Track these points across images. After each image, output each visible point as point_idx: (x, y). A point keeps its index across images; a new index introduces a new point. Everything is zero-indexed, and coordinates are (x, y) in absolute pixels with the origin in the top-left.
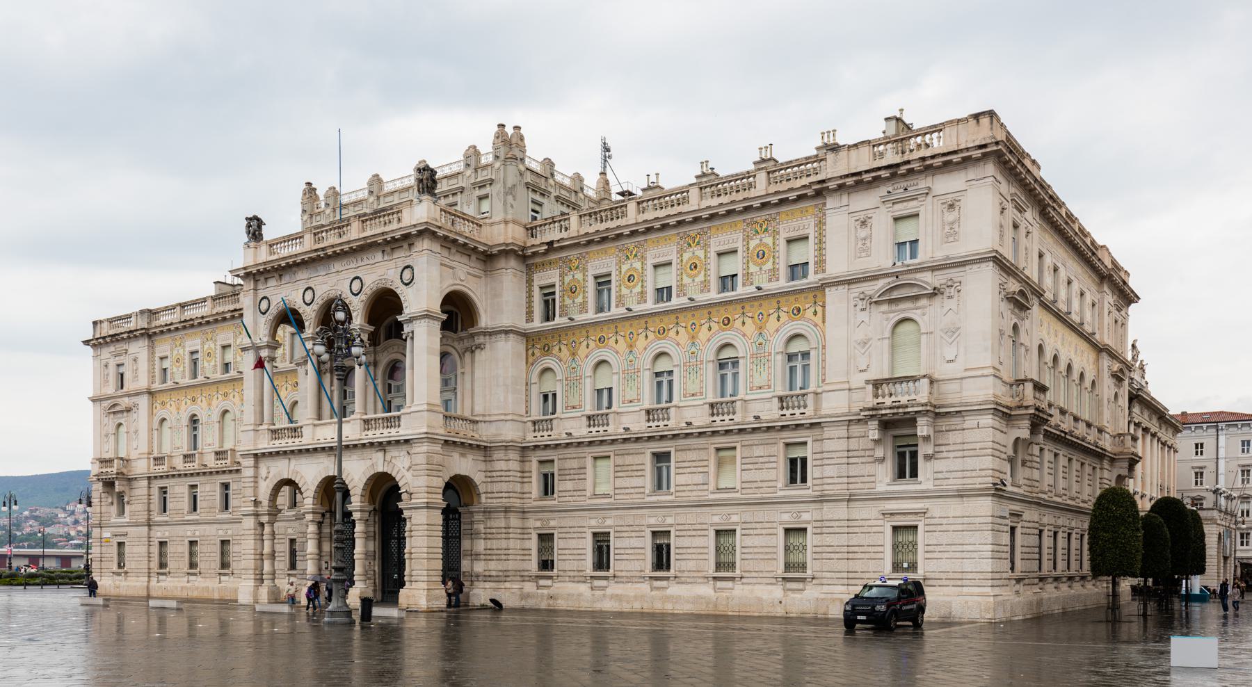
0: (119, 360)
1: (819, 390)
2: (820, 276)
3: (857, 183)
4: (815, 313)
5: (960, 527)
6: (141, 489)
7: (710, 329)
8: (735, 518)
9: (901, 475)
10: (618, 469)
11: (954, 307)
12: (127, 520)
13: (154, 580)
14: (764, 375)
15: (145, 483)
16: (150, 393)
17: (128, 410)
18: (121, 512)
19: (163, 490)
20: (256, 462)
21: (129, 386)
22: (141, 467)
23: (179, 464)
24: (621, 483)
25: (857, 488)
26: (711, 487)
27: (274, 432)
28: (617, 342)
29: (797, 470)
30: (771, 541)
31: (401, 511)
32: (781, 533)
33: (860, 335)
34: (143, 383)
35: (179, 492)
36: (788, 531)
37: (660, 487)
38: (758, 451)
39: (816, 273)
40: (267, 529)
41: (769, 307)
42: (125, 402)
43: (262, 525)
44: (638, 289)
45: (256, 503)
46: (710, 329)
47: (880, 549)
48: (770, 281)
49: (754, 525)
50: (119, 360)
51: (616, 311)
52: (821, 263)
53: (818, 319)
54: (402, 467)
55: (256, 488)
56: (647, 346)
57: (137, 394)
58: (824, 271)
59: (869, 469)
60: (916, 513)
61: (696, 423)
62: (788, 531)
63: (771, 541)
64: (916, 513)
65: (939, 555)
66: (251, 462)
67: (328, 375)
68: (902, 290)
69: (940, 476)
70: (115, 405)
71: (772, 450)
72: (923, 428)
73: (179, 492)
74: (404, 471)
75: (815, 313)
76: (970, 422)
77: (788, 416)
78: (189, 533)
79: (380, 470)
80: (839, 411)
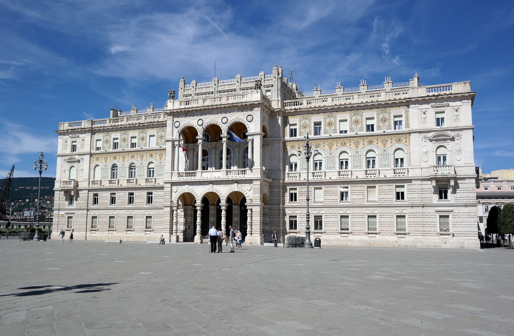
0: (73, 140)
1: (409, 168)
2: (408, 129)
3: (436, 99)
4: (406, 141)
5: (466, 216)
6: (83, 194)
7: (364, 144)
8: (376, 211)
9: (441, 197)
10: (326, 193)
11: (459, 143)
12: (75, 207)
13: (89, 233)
14: (386, 162)
15: (87, 191)
16: (91, 155)
17: (79, 161)
18: (71, 203)
19: (96, 195)
20: (172, 186)
21: (79, 150)
22: (83, 185)
23: (106, 184)
24: (326, 197)
25: (425, 202)
26: (366, 200)
27: (179, 173)
28: (324, 146)
29: (400, 196)
30: (392, 220)
31: (220, 207)
32: (395, 217)
33: (424, 150)
34: (87, 149)
35: (104, 197)
36: (398, 217)
37: (342, 199)
38: (356, 188)
39: (406, 128)
40: (175, 212)
41: (388, 138)
42: (77, 157)
43: (173, 211)
44: (333, 128)
45: (171, 202)
46: (364, 144)
47: (435, 223)
48: (388, 129)
49: (384, 214)
50: (73, 140)
51: (323, 135)
52: (407, 125)
53: (407, 143)
54: (245, 189)
55: (171, 196)
56: (337, 148)
57: (84, 155)
58: (409, 128)
59: (429, 196)
60: (449, 212)
61: (332, 178)
62: (398, 217)
63: (392, 220)
64: (449, 212)
65: (458, 226)
66: (169, 185)
67: (192, 152)
68: (441, 137)
69: (457, 199)
70: (70, 159)
71: (391, 187)
72: (452, 183)
73: (104, 197)
74: (248, 191)
75: (406, 141)
76: (467, 181)
77: (398, 176)
78: (110, 213)
79: (236, 190)
80: (418, 176)
